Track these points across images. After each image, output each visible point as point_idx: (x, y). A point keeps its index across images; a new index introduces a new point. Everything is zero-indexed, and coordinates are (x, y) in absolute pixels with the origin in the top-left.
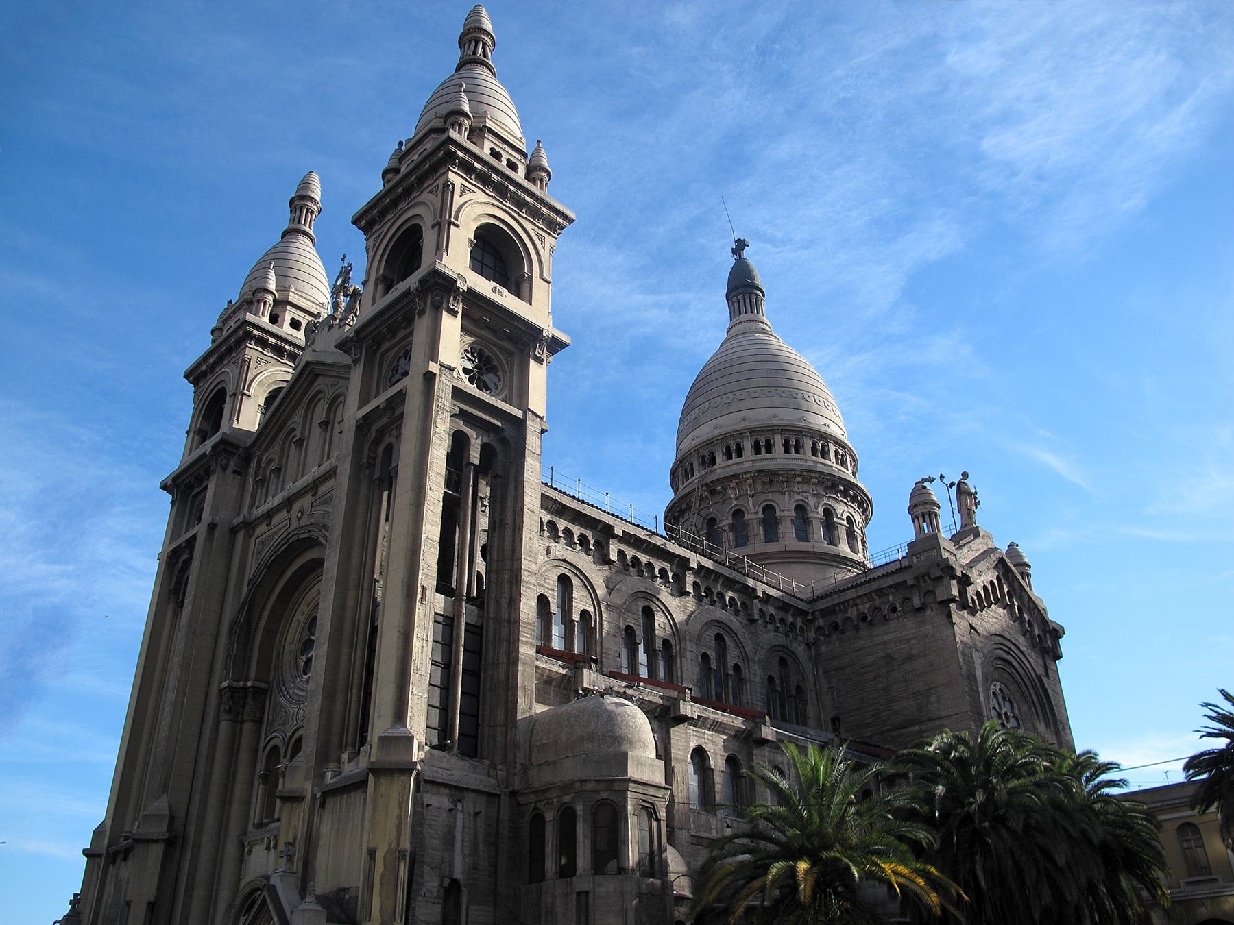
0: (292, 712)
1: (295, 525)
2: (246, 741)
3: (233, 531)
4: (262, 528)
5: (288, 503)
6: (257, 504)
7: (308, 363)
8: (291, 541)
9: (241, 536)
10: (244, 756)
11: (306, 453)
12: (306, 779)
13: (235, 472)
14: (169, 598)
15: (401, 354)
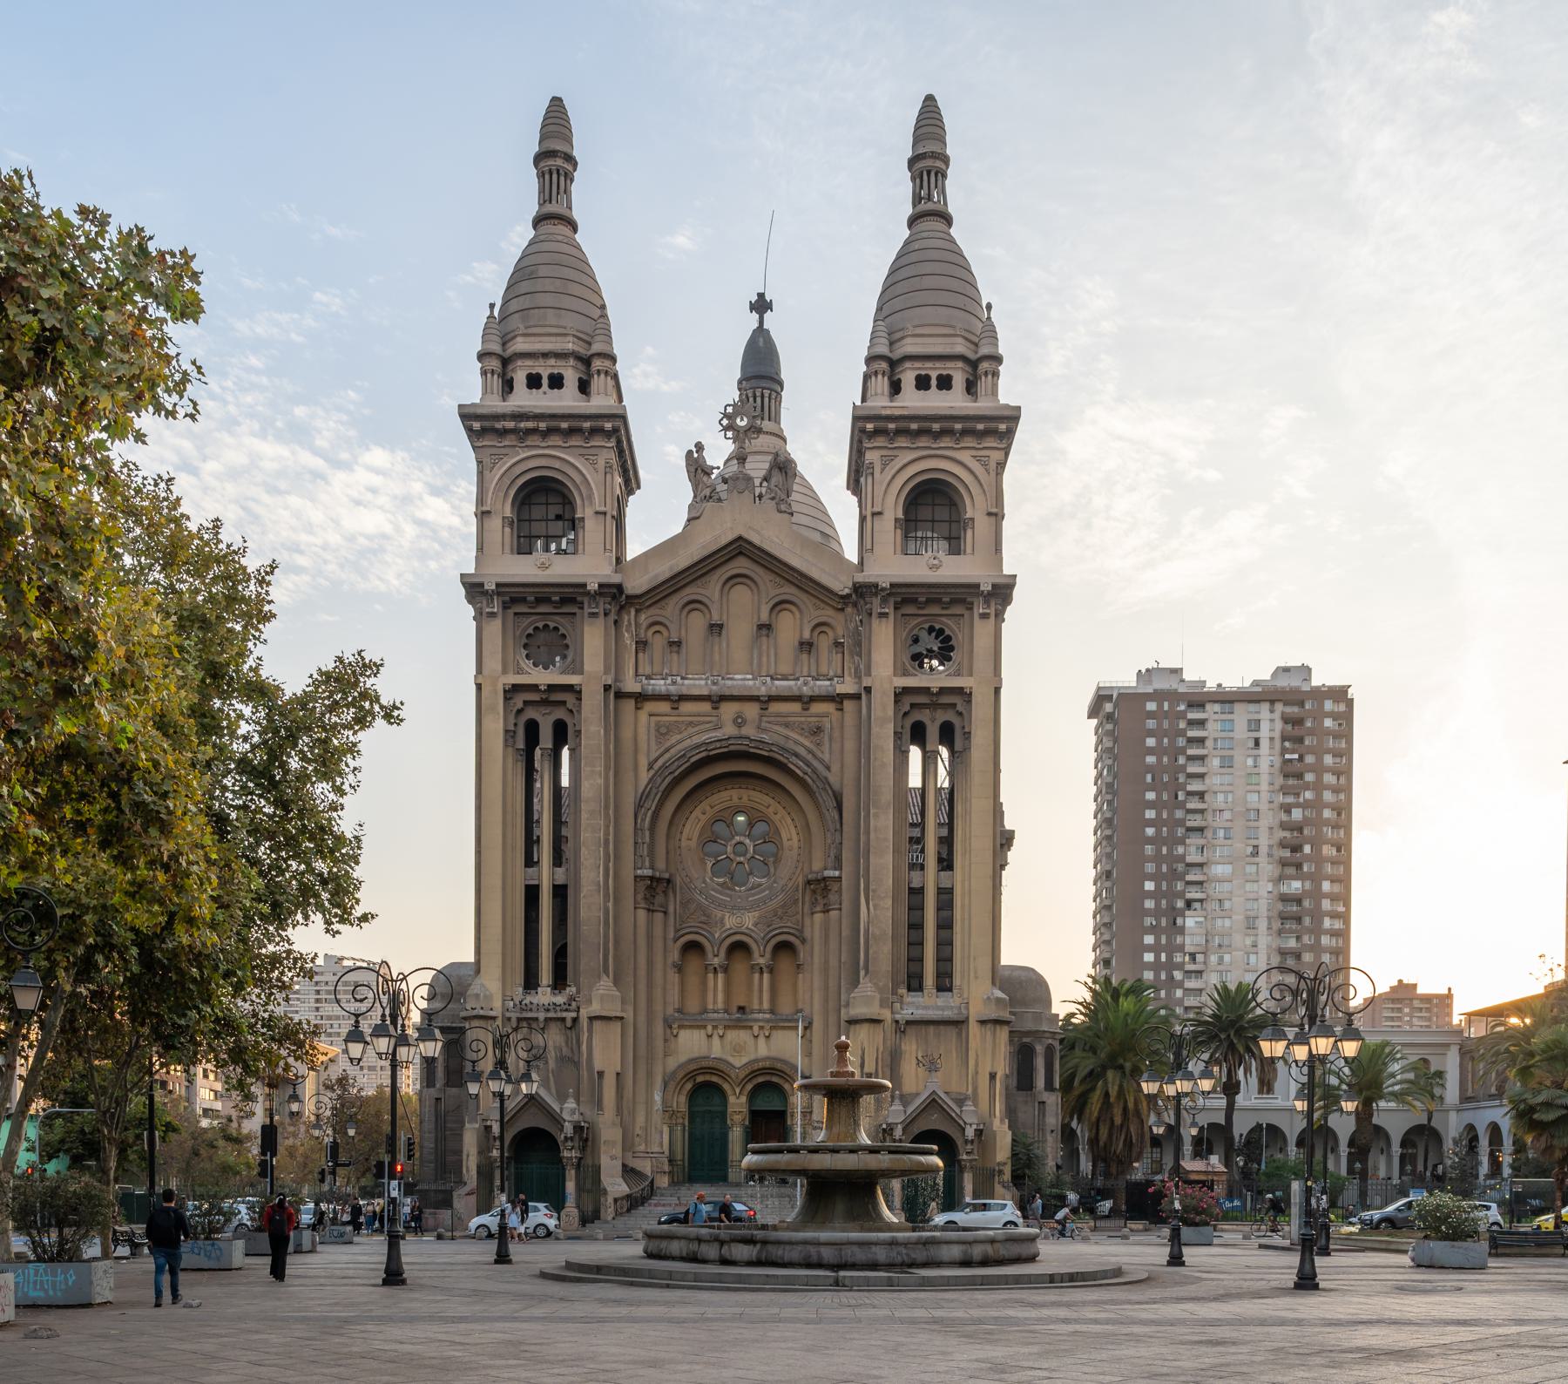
0: (719, 914)
1: (729, 730)
2: (658, 931)
3: (620, 695)
4: (664, 707)
5: (717, 700)
6: (641, 671)
7: (740, 538)
8: (732, 748)
9: (629, 705)
10: (659, 944)
11: (728, 645)
12: (881, 1006)
13: (616, 622)
14: (506, 741)
15: (926, 626)
